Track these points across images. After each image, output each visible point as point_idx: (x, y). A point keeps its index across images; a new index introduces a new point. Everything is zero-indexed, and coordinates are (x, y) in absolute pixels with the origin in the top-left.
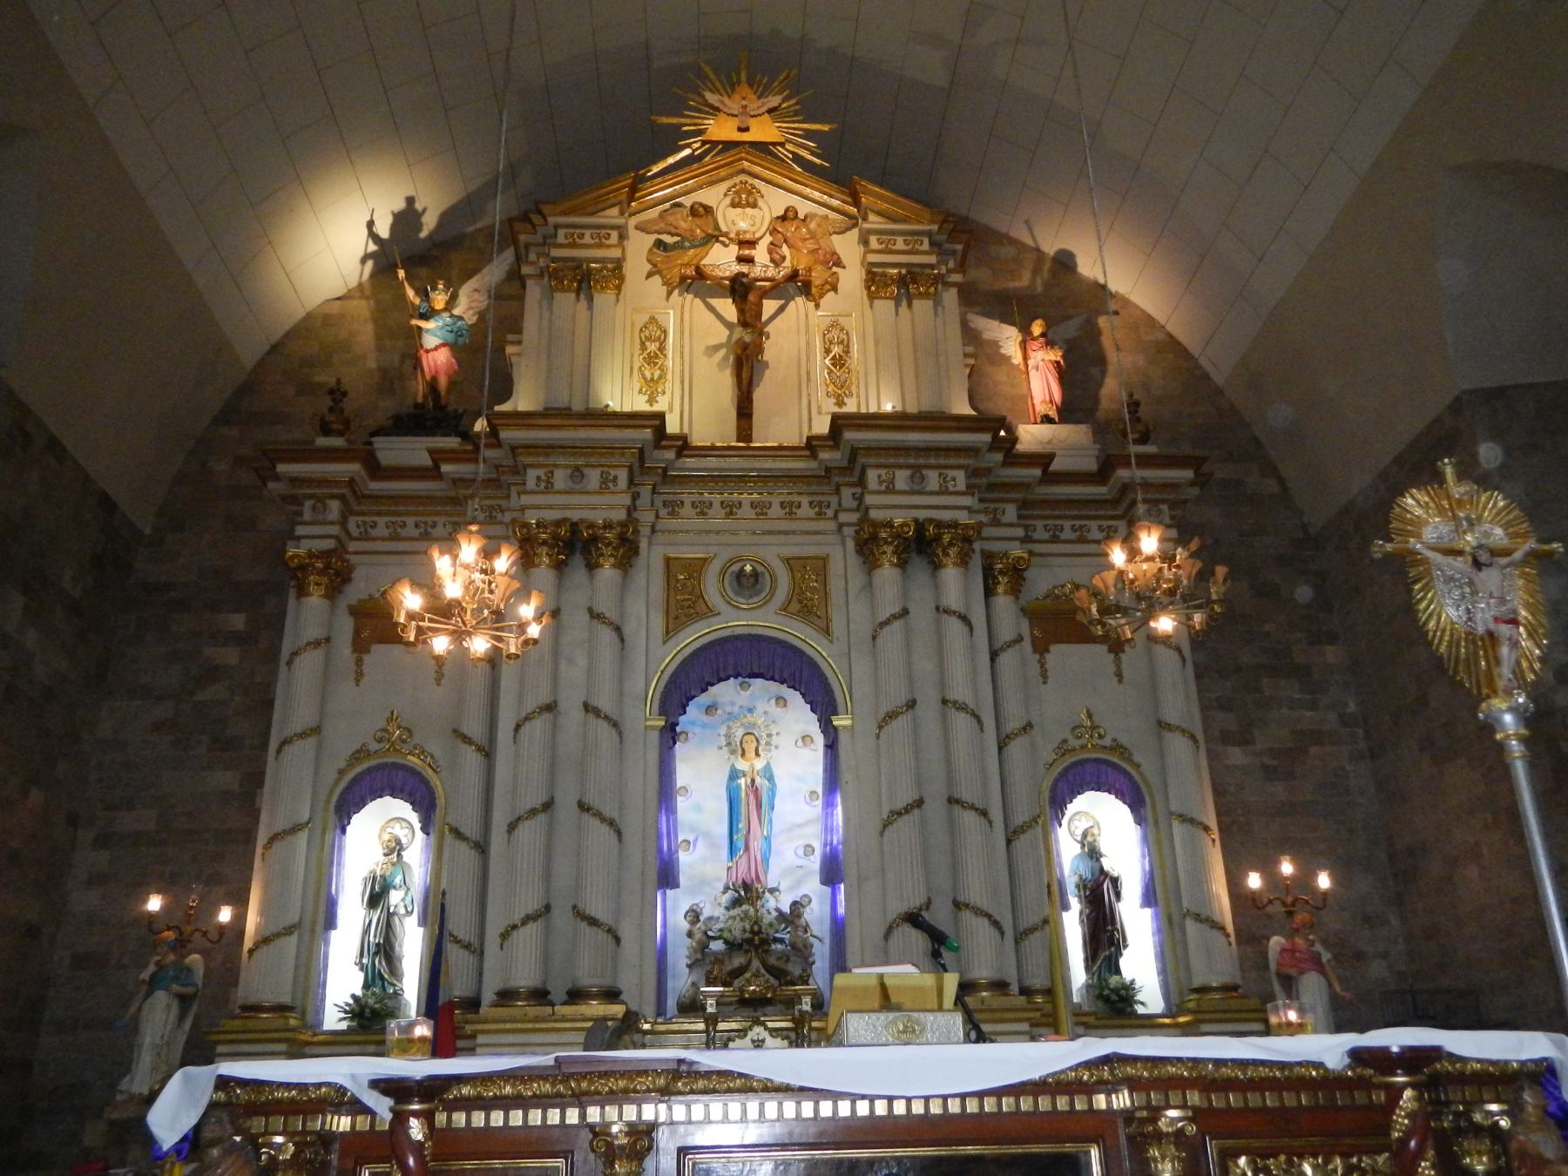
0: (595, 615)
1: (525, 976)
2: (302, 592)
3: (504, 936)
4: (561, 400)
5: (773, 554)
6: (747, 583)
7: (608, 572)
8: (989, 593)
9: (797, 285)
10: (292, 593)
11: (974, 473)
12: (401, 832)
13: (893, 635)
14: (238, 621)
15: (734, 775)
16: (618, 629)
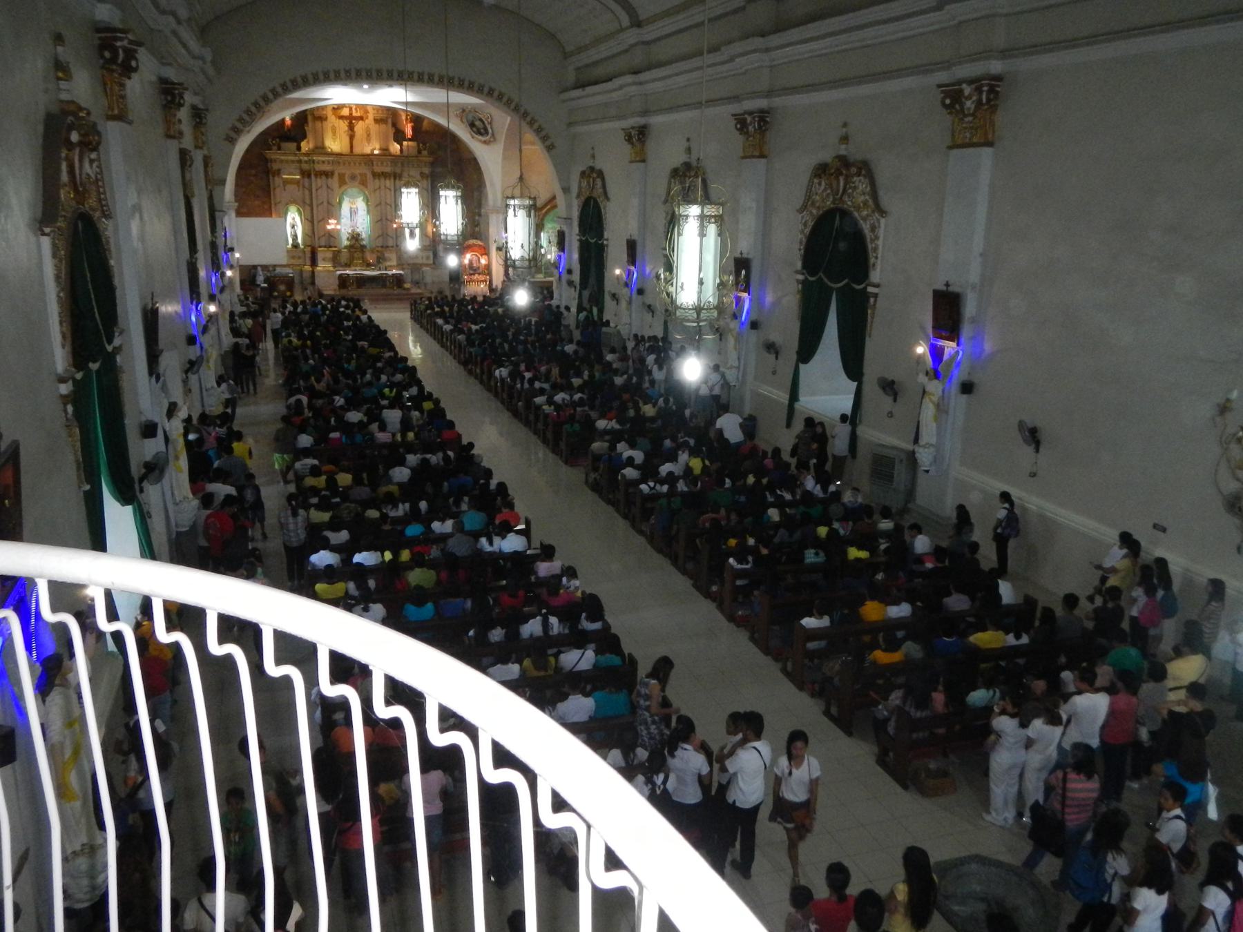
0: (328, 187)
1: (323, 243)
2: (274, 176)
3: (319, 239)
4: (319, 144)
5: (357, 172)
6: (353, 177)
7: (330, 179)
8: (395, 179)
9: (361, 118)
10: (271, 177)
11: (392, 162)
12: (293, 215)
13: (378, 191)
14: (253, 172)
15: (351, 208)
16: (332, 190)
